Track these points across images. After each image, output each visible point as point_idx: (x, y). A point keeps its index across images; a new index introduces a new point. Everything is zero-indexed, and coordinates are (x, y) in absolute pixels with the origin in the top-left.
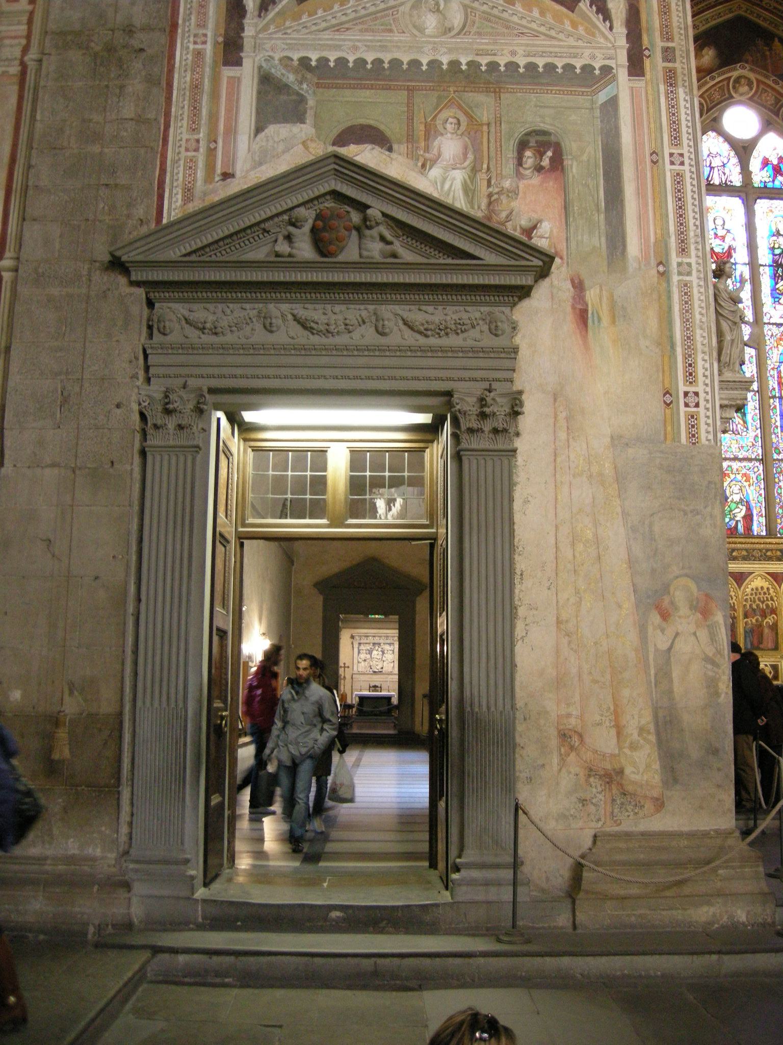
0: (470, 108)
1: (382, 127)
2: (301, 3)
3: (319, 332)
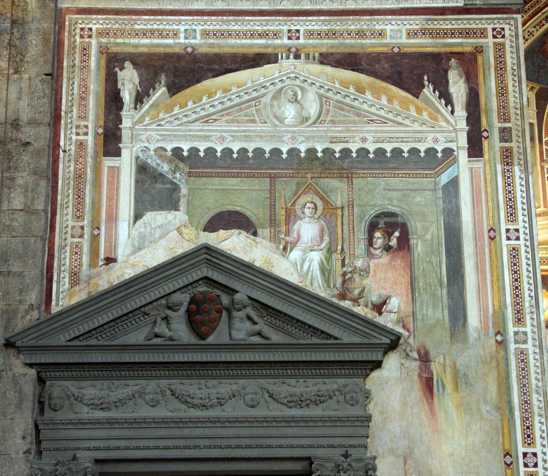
0: (326, 193)
1: (248, 213)
2: (173, 95)
3: (194, 406)
